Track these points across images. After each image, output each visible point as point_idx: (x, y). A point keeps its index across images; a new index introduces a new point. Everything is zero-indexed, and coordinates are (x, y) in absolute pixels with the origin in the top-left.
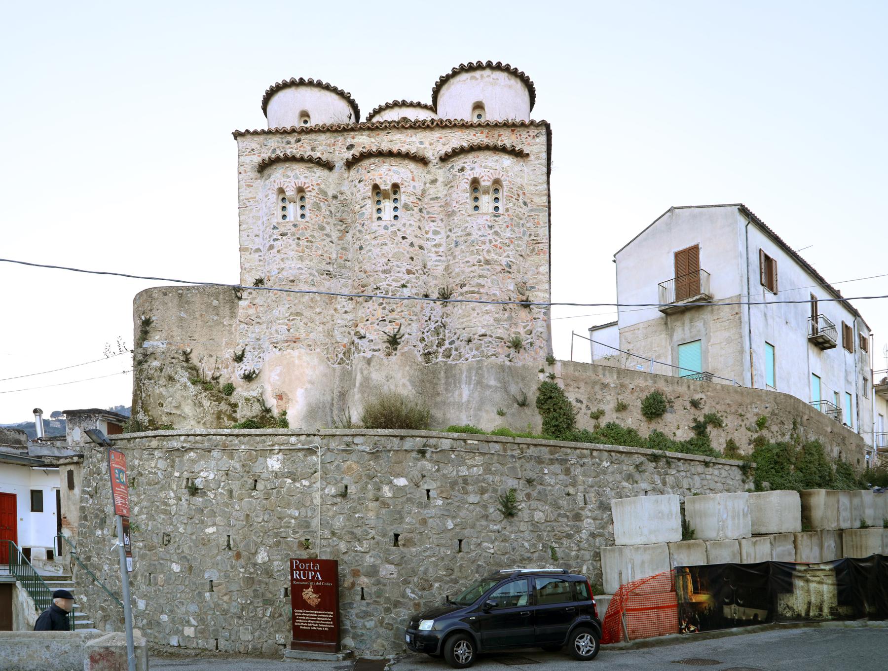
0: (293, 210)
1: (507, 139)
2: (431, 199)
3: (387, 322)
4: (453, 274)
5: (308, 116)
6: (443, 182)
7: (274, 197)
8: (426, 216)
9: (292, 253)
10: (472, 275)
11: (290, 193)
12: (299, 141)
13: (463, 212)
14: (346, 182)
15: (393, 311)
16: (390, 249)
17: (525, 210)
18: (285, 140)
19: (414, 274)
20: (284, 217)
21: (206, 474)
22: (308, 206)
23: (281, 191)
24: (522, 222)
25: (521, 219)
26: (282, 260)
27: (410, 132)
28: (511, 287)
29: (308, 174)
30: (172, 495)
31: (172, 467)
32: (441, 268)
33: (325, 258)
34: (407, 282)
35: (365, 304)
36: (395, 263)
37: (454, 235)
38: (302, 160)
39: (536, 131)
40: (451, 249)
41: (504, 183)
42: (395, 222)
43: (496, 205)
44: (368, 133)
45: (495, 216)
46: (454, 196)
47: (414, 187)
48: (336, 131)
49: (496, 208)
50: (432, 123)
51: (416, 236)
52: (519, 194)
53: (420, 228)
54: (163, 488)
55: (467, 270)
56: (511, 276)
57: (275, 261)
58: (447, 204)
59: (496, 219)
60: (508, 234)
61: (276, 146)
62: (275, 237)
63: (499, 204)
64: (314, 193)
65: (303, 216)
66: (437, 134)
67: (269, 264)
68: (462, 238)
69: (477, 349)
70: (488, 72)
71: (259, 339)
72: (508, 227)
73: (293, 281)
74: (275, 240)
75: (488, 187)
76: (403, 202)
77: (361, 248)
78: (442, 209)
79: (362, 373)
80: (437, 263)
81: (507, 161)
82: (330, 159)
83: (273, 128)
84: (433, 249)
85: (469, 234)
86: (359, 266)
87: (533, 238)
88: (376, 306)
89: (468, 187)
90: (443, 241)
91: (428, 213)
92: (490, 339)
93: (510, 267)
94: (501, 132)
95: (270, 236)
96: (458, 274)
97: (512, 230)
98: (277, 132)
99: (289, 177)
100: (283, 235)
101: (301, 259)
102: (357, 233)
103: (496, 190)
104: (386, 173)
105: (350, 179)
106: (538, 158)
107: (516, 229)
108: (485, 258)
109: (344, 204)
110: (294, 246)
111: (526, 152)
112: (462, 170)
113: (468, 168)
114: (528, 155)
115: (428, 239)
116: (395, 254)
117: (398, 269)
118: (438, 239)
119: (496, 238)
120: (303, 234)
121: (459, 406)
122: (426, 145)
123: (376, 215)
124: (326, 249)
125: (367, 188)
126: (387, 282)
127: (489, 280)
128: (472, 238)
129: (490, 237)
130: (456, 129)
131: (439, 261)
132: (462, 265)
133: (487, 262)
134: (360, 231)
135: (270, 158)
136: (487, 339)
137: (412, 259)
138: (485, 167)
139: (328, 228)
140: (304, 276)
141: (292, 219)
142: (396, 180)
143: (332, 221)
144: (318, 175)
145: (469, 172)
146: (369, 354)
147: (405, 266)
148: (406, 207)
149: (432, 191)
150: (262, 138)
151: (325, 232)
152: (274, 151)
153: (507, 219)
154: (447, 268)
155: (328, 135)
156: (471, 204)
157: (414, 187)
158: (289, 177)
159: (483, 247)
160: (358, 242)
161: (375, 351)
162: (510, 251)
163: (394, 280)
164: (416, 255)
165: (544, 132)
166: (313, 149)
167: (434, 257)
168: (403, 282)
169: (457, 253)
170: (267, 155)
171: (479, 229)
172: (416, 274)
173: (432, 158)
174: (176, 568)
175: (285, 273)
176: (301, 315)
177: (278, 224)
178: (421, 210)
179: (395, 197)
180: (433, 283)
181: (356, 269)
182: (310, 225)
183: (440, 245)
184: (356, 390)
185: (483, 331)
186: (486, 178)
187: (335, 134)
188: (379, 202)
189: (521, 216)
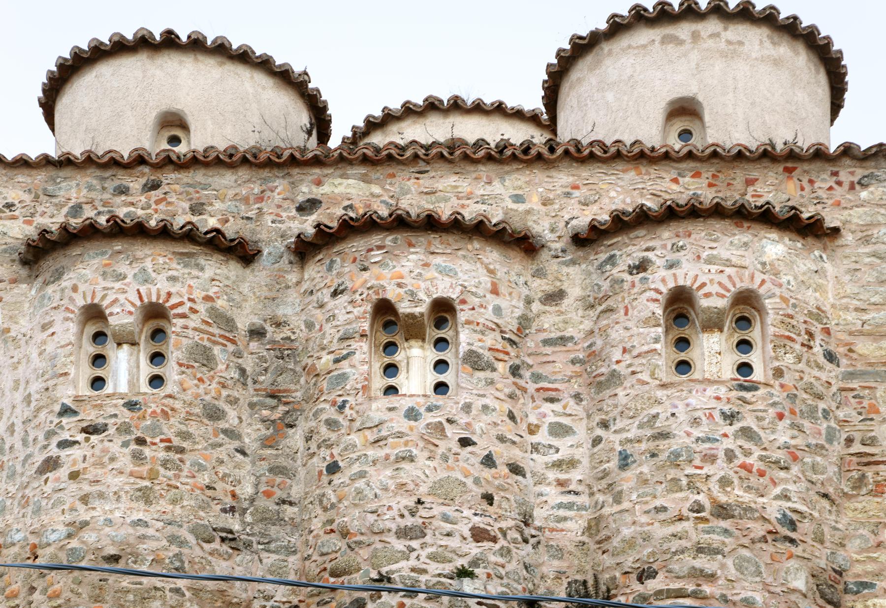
0: (126, 368)
1: (772, 190)
2: (547, 342)
4: (616, 542)
5: (184, 126)
6: (583, 299)
7: (67, 330)
8: (531, 387)
9: (115, 482)
10: (675, 545)
11: (122, 316)
12: (155, 186)
13: (645, 377)
14: (293, 296)
16: (424, 471)
17: (830, 373)
18: (110, 185)
19: (494, 540)
20: (98, 382)
22: (175, 352)
23: (94, 313)
24: (822, 405)
25: (820, 397)
26: (85, 499)
27: (484, 170)
28: (800, 583)
29: (178, 269)
32: (575, 526)
33: (219, 494)
34: (475, 563)
36: (437, 510)
38: (164, 233)
39: (860, 172)
40: (606, 474)
41: (768, 303)
42: (439, 400)
43: (744, 358)
44: (362, 170)
45: (742, 388)
46: (616, 334)
47: (498, 310)
48: (269, 164)
49: (745, 368)
50: (552, 150)
51: (501, 439)
52: (810, 330)
53: (512, 417)
55: (660, 531)
56: (798, 551)
57: (60, 502)
58: (593, 355)
59: (748, 395)
60: (783, 435)
61: (80, 198)
62: (65, 436)
63: (754, 358)
64: (194, 321)
65: (156, 381)
66: (562, 178)
67: (38, 511)
68: (643, 446)
72: (781, 416)
75: (721, 313)
76: (463, 348)
77: (333, 468)
78: (577, 368)
80: (562, 513)
81: (775, 246)
82: (247, 236)
83: (78, 151)
84: (552, 475)
85: (664, 435)
86: (323, 517)
87: (857, 448)
89: (659, 311)
90: (582, 454)
91: (537, 378)
94: (755, 174)
95: (49, 434)
96: (630, 543)
97: (793, 426)
98: (90, 161)
99: (121, 277)
100: (91, 430)
101: (145, 496)
102: (323, 429)
103: (744, 322)
104: (415, 275)
105: (305, 286)
107: (806, 424)
109: (285, 351)
110: (125, 461)
111: (831, 220)
112: (642, 266)
113: (659, 262)
114: (836, 231)
115: (535, 448)
117: (448, 527)
118: (565, 447)
119: (747, 445)
120: (154, 430)
122: (534, 202)
124: (222, 470)
125: (357, 311)
126: (412, 562)
127: (729, 562)
128: (674, 444)
129: (729, 444)
130: (620, 166)
131: (570, 506)
132: (644, 519)
133: (722, 511)
134: (332, 424)
135: (64, 228)
137: (489, 499)
138: (710, 261)
139: (232, 414)
140: (152, 545)
141: (123, 388)
142: (445, 289)
143: (246, 395)
144: (209, 273)
145: (663, 273)
147: (469, 518)
148: (474, 361)
149: (549, 321)
150: (40, 177)
151: (223, 425)
152: (77, 210)
153: (779, 396)
154: (594, 527)
155: (244, 173)
156: (665, 356)
157: (498, 310)
158: (121, 277)
159: (707, 470)
160: (324, 452)
162: (792, 483)
163: (433, 557)
164: (500, 488)
166: (197, 209)
167: (554, 495)
168: (460, 562)
169: (625, 486)
170: (52, 220)
171: (696, 422)
172: (502, 542)
173: (548, 236)
175: (90, 537)
177: (78, 400)
178: (515, 371)
179: (441, 334)
180: (550, 566)
181: (316, 525)
182: (178, 405)
183: (572, 463)
186: (714, 289)
187: (265, 173)
188: (390, 347)
189: (819, 388)
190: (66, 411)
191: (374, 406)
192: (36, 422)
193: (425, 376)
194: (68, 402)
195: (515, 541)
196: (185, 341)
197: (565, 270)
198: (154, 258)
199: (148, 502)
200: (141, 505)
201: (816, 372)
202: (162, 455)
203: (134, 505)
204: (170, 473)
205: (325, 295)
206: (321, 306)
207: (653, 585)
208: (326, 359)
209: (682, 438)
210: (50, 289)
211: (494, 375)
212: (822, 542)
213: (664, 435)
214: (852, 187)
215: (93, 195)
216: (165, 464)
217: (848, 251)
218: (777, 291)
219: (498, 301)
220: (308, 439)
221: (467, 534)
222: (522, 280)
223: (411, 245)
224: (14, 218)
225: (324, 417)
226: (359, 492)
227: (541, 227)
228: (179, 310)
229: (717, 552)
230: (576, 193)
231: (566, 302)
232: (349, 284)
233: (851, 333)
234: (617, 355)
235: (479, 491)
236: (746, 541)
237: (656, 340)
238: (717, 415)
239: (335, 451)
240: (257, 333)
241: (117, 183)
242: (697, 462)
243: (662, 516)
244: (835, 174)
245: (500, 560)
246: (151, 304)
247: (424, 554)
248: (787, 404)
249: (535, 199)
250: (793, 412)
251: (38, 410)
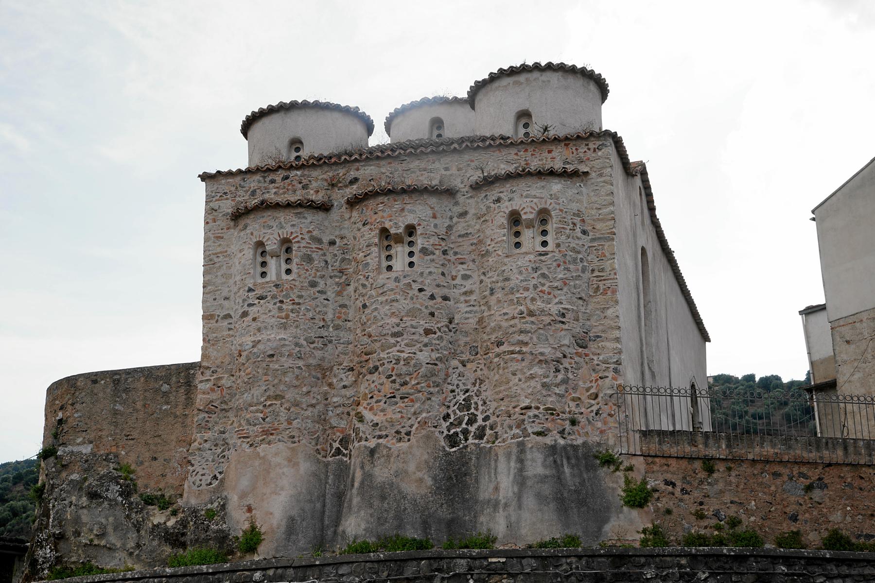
3: (398, 399)
4: (488, 329)
7: (249, 253)
10: (511, 330)
12: (287, 178)
15: (405, 383)
16: (404, 304)
19: (435, 333)
22: (295, 261)
23: (260, 244)
24: (580, 256)
25: (579, 252)
29: (296, 221)
35: (368, 377)
37: (489, 281)
39: (599, 143)
43: (544, 238)
46: (488, 232)
49: (544, 244)
51: (438, 286)
53: (443, 274)
56: (566, 327)
58: (480, 242)
69: (518, 427)
70: (536, 74)
71: (224, 432)
72: (559, 266)
73: (272, 356)
74: (250, 305)
76: (420, 246)
77: (365, 306)
79: (362, 468)
85: (507, 279)
88: (383, 379)
92: (536, 412)
93: (563, 315)
95: (244, 300)
96: (493, 330)
97: (565, 269)
100: (261, 298)
101: (284, 326)
102: (360, 288)
103: (544, 222)
106: (601, 175)
107: (572, 267)
108: (528, 308)
110: (275, 312)
111: (583, 168)
116: (409, 311)
117: (413, 330)
120: (287, 296)
123: (385, 264)
125: (373, 233)
126: (398, 348)
128: (512, 284)
132: (499, 318)
133: (531, 314)
134: (364, 286)
136: (531, 413)
137: (432, 314)
139: (322, 283)
140: (288, 348)
141: (274, 278)
146: (372, 444)
149: (460, 227)
150: (238, 179)
153: (558, 255)
157: (436, 226)
159: (526, 294)
160: (361, 299)
161: (380, 437)
162: (562, 296)
163: (407, 345)
164: (438, 309)
165: (610, 142)
172: (439, 334)
175: (261, 346)
176: (283, 398)
178: (445, 252)
179: (411, 239)
184: (354, 491)
185: (526, 402)
187: (334, 168)
188: (388, 247)
190: (250, 290)
191: (381, 277)
192: (238, 294)
193: (404, 260)
194: (251, 286)
195: (445, 332)
196: (299, 253)
197: (468, 201)
198: (282, 216)
199: (285, 329)
200: (282, 331)
201: (577, 242)
202: (291, 307)
203: (279, 331)
204: (294, 315)
205: (360, 225)
206: (359, 230)
207: (503, 348)
208: (362, 254)
209: (516, 279)
210: (242, 234)
211: (434, 257)
212: (578, 320)
213: (507, 279)
214: (595, 151)
215: (260, 185)
216: (292, 311)
217: (593, 181)
218: (557, 207)
219: (436, 221)
220: (355, 291)
221: (422, 332)
222: (448, 209)
223: (395, 201)
224: (227, 199)
225: (361, 282)
226: (375, 317)
227: (457, 183)
228: (296, 240)
229: (529, 332)
230: (473, 164)
231: (469, 217)
232: (369, 220)
233: (594, 220)
234: (489, 242)
235: (427, 312)
236: (541, 326)
237: (504, 235)
238: (530, 269)
239: (366, 298)
240: (332, 243)
241: (270, 178)
242: (521, 291)
243: (506, 317)
244: (587, 145)
245: (437, 342)
246: (284, 238)
247: (403, 343)
248: (562, 260)
249: (454, 168)
250: (565, 262)
251: (239, 289)
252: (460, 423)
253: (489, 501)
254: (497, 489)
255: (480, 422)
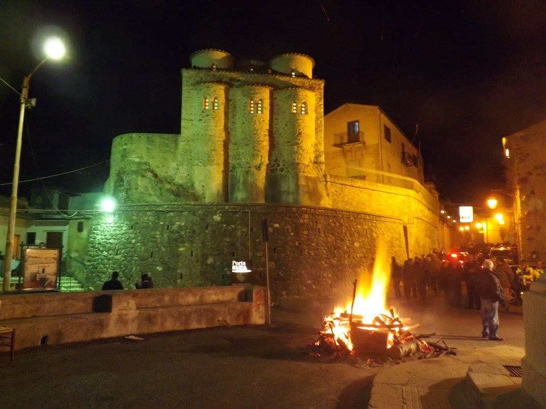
21: (179, 223)
30: (158, 233)
31: (159, 220)
54: (152, 230)
74: (203, 117)
121: (288, 193)
174: (159, 269)
252: (274, 166)
253: (285, 191)
254: (289, 188)
255: (281, 166)
